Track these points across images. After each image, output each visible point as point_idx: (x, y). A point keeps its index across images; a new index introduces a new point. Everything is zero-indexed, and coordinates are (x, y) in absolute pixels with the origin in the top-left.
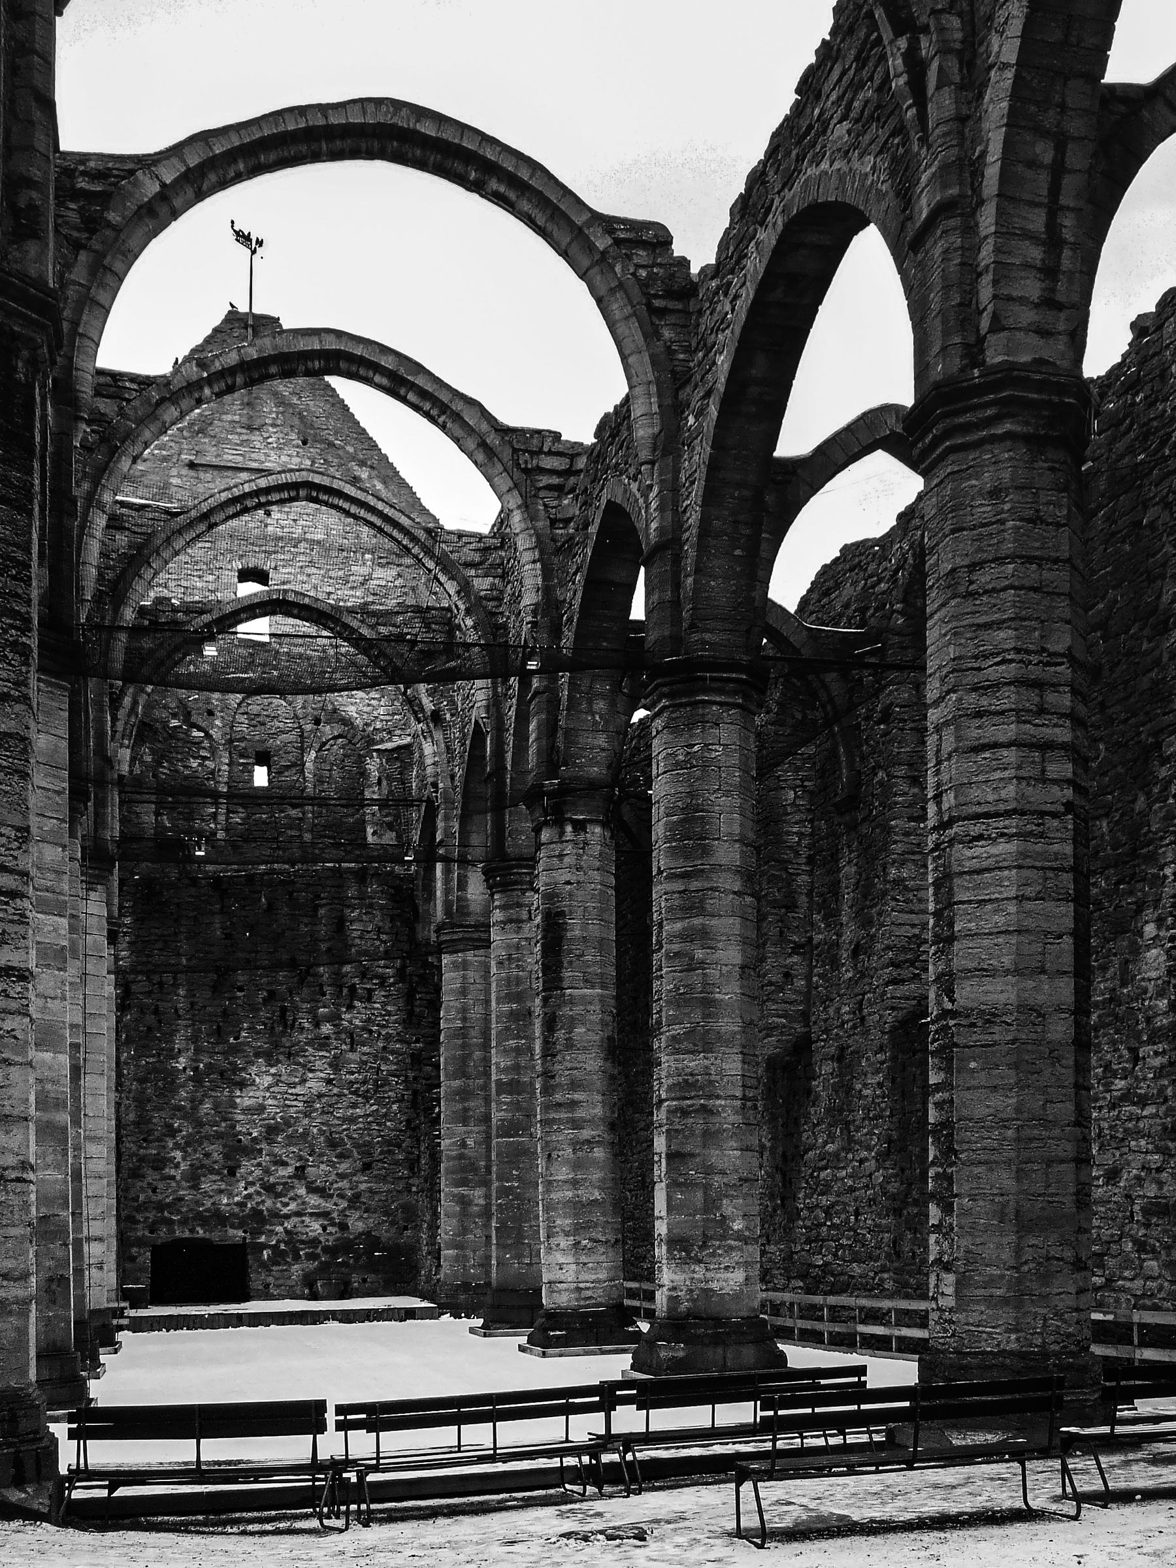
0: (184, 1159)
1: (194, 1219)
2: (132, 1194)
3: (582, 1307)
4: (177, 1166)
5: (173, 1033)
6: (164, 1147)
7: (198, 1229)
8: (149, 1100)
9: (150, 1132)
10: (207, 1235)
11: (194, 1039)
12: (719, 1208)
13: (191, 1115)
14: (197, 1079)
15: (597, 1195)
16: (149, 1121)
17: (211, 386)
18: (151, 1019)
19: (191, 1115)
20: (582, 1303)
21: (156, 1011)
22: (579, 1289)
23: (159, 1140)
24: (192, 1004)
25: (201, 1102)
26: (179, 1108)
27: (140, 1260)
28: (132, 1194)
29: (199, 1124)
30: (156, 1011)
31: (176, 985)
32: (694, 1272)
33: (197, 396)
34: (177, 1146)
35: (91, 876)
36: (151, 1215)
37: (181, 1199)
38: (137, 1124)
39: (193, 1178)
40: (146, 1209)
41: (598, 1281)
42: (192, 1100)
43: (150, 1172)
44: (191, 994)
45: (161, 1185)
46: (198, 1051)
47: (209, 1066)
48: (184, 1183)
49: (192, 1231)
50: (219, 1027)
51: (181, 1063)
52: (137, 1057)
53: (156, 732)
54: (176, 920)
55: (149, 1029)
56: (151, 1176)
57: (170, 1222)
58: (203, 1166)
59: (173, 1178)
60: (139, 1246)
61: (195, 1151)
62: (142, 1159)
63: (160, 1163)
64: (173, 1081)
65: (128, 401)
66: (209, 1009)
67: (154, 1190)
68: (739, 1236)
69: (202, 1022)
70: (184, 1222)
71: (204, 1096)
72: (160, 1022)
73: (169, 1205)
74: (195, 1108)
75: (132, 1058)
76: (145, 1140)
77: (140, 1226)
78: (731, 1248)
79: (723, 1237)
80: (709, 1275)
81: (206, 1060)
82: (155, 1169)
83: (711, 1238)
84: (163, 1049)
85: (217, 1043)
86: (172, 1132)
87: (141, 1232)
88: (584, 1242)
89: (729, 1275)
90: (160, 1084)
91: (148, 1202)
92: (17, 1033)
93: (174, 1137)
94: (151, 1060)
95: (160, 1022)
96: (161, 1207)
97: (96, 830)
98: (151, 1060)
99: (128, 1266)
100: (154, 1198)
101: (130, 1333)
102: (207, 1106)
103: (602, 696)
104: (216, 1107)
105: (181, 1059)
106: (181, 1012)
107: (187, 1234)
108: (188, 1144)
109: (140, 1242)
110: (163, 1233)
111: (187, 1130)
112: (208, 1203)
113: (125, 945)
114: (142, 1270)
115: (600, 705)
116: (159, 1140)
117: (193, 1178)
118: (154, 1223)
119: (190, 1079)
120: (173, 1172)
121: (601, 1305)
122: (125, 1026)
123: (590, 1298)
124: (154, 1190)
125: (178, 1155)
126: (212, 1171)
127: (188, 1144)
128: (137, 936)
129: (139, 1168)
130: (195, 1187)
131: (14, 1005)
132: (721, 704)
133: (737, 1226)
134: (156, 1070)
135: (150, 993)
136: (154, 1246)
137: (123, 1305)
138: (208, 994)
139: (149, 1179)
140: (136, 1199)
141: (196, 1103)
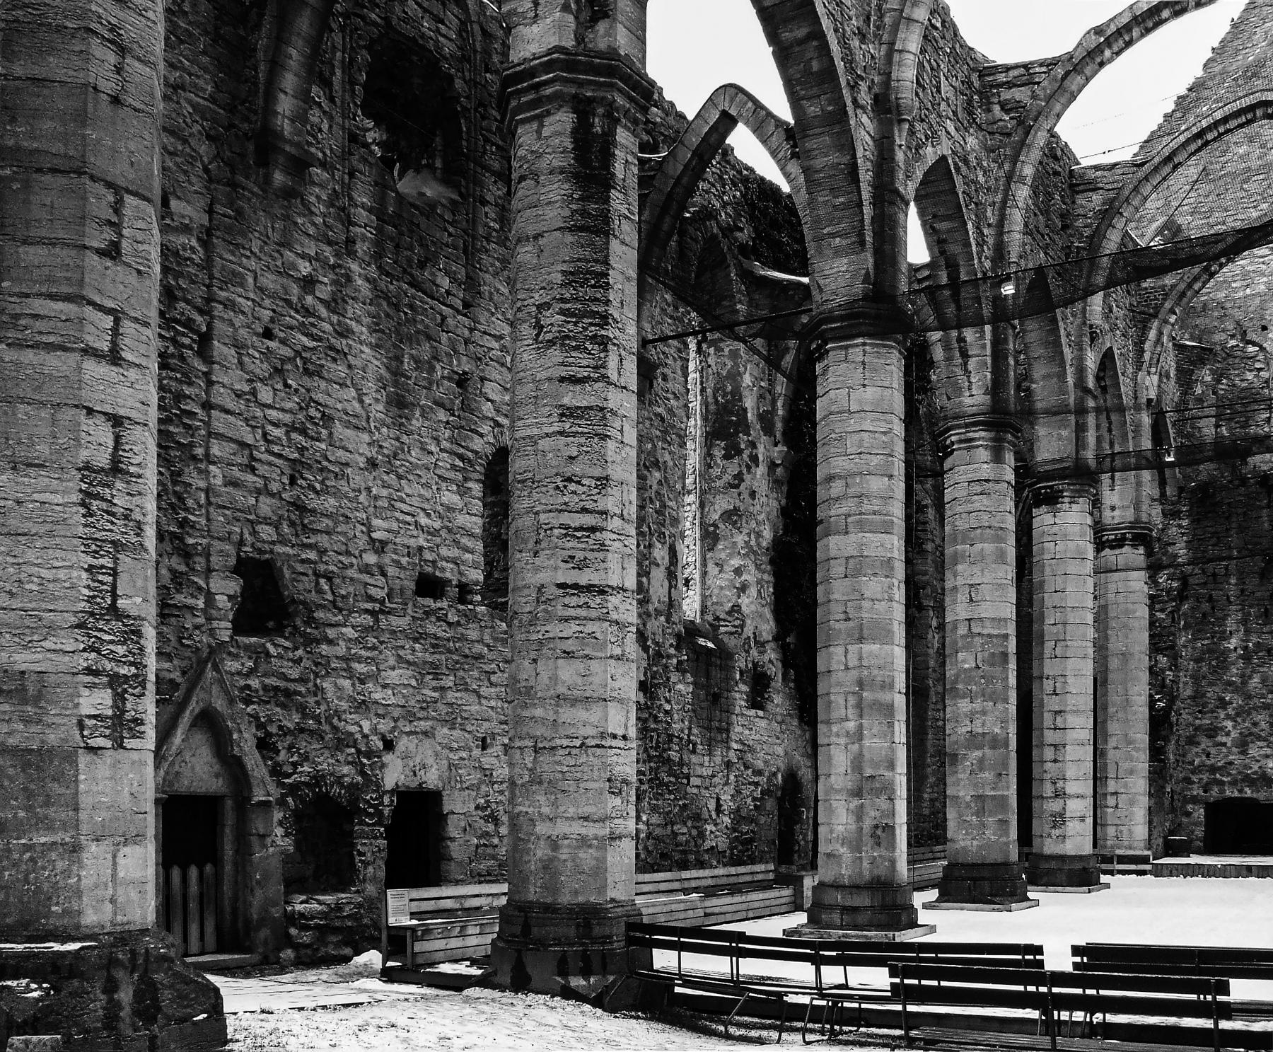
0: (1234, 727)
1: (1243, 780)
2: (1189, 758)
4: (1228, 734)
5: (1224, 618)
6: (1216, 718)
7: (1247, 789)
8: (1204, 678)
9: (1205, 705)
10: (1255, 795)
11: (1244, 621)
13: (1240, 689)
14: (1247, 657)
16: (1204, 695)
18: (1206, 606)
19: (1240, 689)
21: (1210, 600)
23: (1212, 711)
24: (1242, 591)
25: (1250, 677)
26: (1230, 683)
27: (1196, 815)
28: (1189, 758)
29: (1249, 697)
30: (1210, 600)
31: (1227, 575)
34: (1228, 717)
35: (1076, 491)
36: (1205, 777)
37: (1231, 763)
38: (1193, 698)
39: (1243, 745)
40: (1200, 772)
42: (1242, 676)
43: (1204, 739)
44: (1241, 581)
45: (1213, 751)
46: (1247, 632)
47: (1257, 645)
48: (1234, 750)
49: (1241, 791)
50: (1266, 610)
51: (1233, 642)
52: (1195, 639)
53: (1215, 355)
54: (1227, 518)
55: (1204, 615)
56: (1205, 742)
57: (1222, 783)
58: (1251, 734)
59: (1224, 744)
60: (1194, 803)
61: (1244, 721)
62: (1197, 729)
63: (1212, 732)
64: (1225, 660)
65: (1038, 83)
66: (1258, 594)
67: (1208, 755)
69: (1251, 607)
70: (1234, 783)
71: (1253, 671)
72: (1213, 608)
73: (1220, 768)
74: (1244, 683)
75: (1189, 641)
76: (1200, 712)
77: (1195, 786)
81: (1255, 640)
82: (1209, 737)
84: (1216, 632)
85: (1265, 624)
86: (1223, 704)
87: (1196, 791)
90: (1214, 663)
91: (1203, 765)
92: (598, 635)
93: (1225, 709)
94: (1206, 642)
95: (1213, 608)
96: (1213, 769)
97: (1077, 452)
98: (1206, 642)
99: (1185, 820)
100: (1208, 762)
102: (1256, 680)
104: (1263, 681)
105: (1233, 641)
106: (1232, 599)
107: (1236, 794)
108: (1238, 715)
109: (1195, 800)
110: (1215, 792)
111: (1238, 701)
112: (1256, 768)
113: (1183, 544)
114: (1196, 824)
116: (1212, 711)
117: (1243, 745)
118: (1207, 784)
119: (1241, 657)
120: (1224, 739)
122: (1184, 614)
124: (1208, 755)
125: (1229, 724)
126: (1259, 738)
127: (1238, 715)
128: (1194, 536)
129: (1194, 736)
130: (1244, 753)
131: (594, 614)
134: (1210, 651)
135: (1205, 583)
136: (1207, 803)
137: (1146, 853)
138: (1256, 580)
139: (1203, 746)
140: (1192, 763)
141: (1245, 678)
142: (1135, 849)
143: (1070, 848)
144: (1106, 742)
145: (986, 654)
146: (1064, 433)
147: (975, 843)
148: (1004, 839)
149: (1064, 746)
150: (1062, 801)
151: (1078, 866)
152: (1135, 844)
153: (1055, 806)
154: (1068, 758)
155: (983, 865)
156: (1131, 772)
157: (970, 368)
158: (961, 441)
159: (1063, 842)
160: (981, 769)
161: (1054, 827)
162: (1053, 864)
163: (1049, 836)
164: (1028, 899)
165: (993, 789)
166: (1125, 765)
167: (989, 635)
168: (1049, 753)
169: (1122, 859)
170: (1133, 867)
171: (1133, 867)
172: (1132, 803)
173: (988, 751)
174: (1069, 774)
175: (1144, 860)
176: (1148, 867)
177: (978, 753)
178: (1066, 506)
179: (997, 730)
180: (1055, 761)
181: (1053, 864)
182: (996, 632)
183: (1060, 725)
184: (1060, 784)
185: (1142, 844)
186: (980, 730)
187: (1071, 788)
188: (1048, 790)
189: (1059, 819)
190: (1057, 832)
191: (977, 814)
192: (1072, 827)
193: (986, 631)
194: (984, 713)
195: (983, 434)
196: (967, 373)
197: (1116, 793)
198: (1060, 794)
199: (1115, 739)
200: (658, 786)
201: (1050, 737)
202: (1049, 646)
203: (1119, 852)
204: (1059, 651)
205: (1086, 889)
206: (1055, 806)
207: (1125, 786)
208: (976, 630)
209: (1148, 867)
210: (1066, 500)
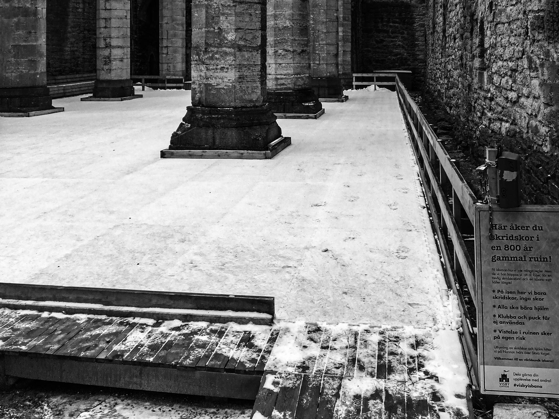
3: (277, 89)
12: (217, 23)
15: (288, 23)
20: (279, 87)
22: (277, 79)
32: (201, 71)
41: (288, 74)
68: (233, 45)
78: (226, 54)
79: (220, 45)
80: (210, 73)
83: (211, 45)
88: (280, 51)
89: (224, 74)
101: (184, 90)
121: (290, 89)
123: (283, 84)
133: (231, 36)
137: (181, 77)
142: (177, 75)
143: (113, 76)
144: (162, 21)
147: (13, 74)
148: (33, 72)
149: (110, 19)
150: (109, 50)
151: (119, 86)
152: (177, 73)
153: (106, 52)
154: (113, 25)
155: (17, 88)
156: (175, 35)
159: (110, 72)
160: (17, 29)
161: (105, 64)
162: (105, 85)
163: (103, 69)
164: (54, 108)
165: (25, 41)
166: (171, 32)
168: (102, 23)
169: (170, 81)
170: (174, 85)
171: (174, 85)
172: (175, 51)
173: (22, 19)
174: (112, 35)
175: (180, 81)
176: (182, 85)
177: (15, 20)
179: (28, 5)
180: (106, 27)
181: (105, 85)
183: (108, 8)
184: (108, 40)
185: (181, 73)
187: (114, 43)
188: (102, 44)
189: (108, 60)
190: (106, 67)
191: (14, 57)
192: (115, 64)
197: (167, 47)
198: (108, 46)
199: (166, 18)
201: (103, 14)
203: (168, 77)
205: (120, 99)
206: (106, 52)
207: (172, 43)
209: (182, 85)
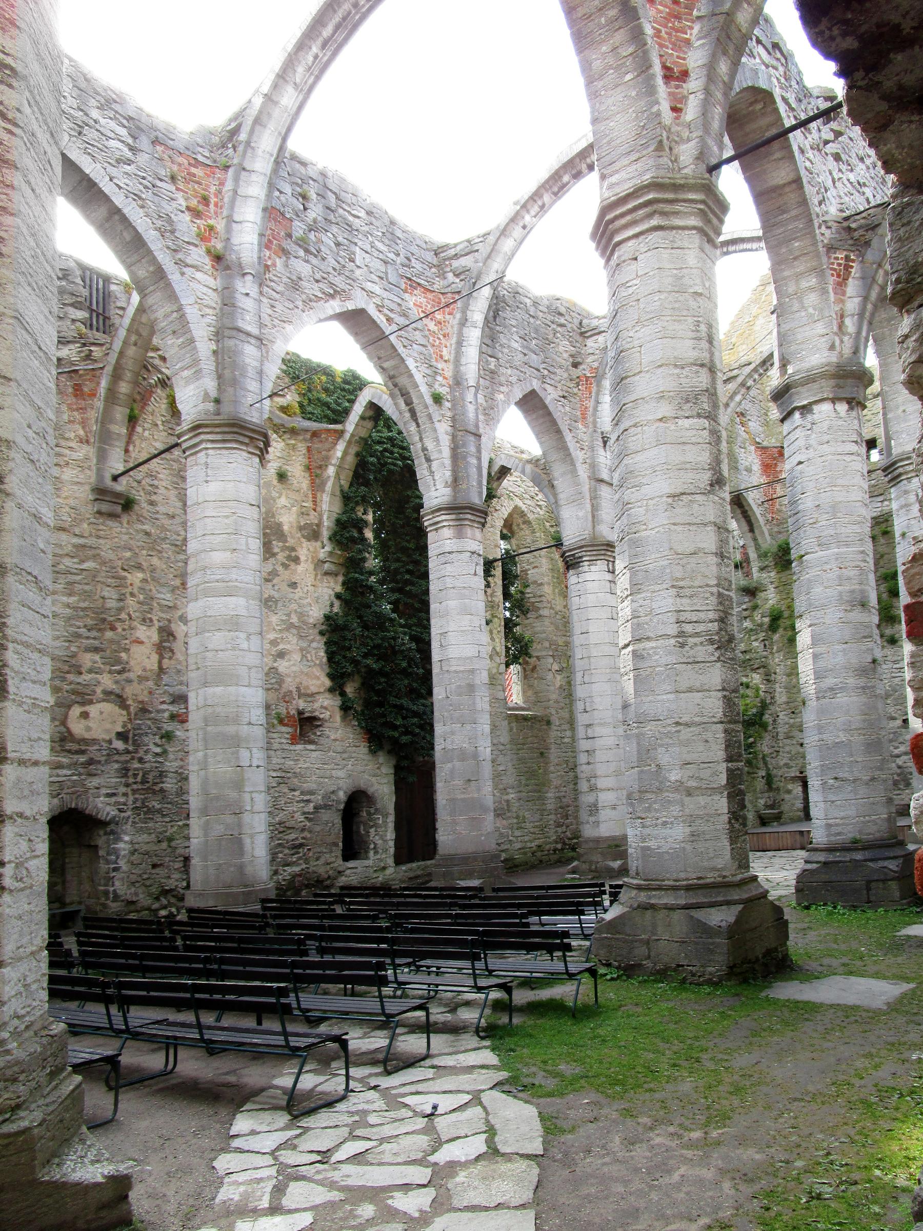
17: (528, 212)
33: (521, 224)
97: (594, 527)
103: (811, 289)
115: (812, 299)
132: (636, 236)
145: (453, 686)
146: (581, 514)
157: (433, 469)
158: (431, 525)
167: (456, 672)
173: (458, 764)
178: (586, 568)
182: (462, 668)
186: (450, 747)
193: (453, 669)
194: (453, 733)
195: (444, 517)
196: (432, 473)
200: (145, 813)
202: (579, 676)
204: (586, 679)
208: (445, 669)
210: (586, 563)
